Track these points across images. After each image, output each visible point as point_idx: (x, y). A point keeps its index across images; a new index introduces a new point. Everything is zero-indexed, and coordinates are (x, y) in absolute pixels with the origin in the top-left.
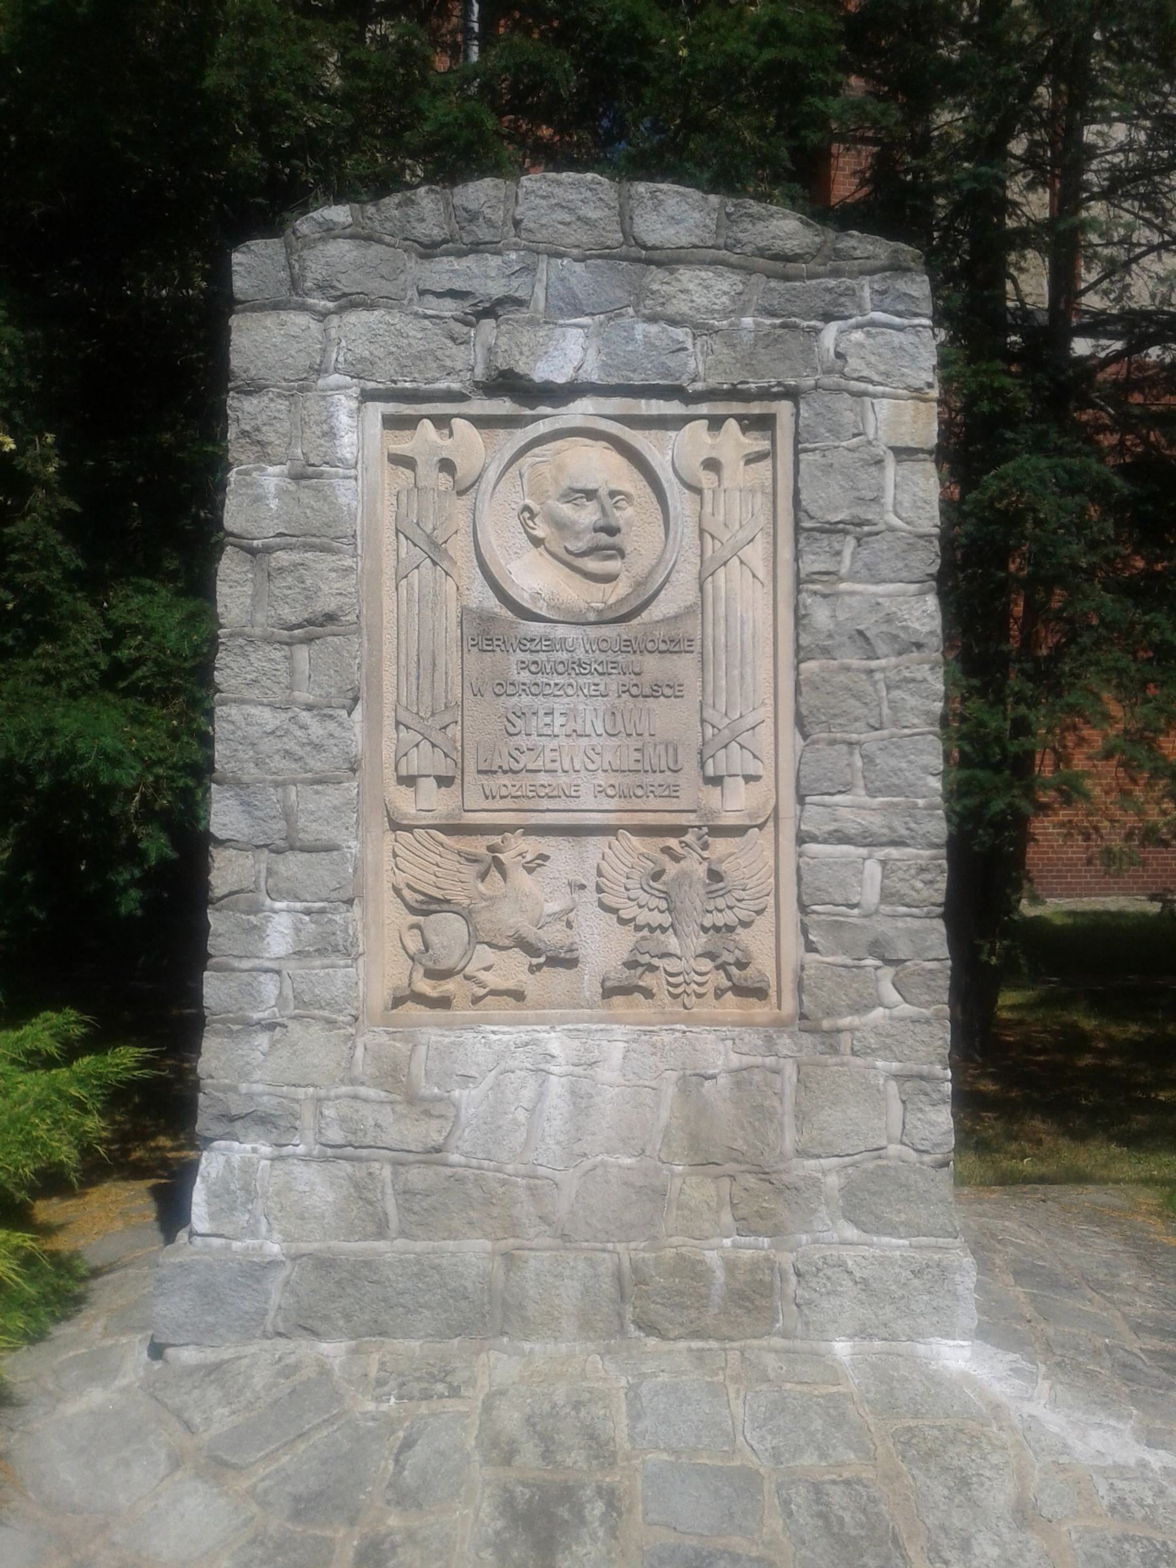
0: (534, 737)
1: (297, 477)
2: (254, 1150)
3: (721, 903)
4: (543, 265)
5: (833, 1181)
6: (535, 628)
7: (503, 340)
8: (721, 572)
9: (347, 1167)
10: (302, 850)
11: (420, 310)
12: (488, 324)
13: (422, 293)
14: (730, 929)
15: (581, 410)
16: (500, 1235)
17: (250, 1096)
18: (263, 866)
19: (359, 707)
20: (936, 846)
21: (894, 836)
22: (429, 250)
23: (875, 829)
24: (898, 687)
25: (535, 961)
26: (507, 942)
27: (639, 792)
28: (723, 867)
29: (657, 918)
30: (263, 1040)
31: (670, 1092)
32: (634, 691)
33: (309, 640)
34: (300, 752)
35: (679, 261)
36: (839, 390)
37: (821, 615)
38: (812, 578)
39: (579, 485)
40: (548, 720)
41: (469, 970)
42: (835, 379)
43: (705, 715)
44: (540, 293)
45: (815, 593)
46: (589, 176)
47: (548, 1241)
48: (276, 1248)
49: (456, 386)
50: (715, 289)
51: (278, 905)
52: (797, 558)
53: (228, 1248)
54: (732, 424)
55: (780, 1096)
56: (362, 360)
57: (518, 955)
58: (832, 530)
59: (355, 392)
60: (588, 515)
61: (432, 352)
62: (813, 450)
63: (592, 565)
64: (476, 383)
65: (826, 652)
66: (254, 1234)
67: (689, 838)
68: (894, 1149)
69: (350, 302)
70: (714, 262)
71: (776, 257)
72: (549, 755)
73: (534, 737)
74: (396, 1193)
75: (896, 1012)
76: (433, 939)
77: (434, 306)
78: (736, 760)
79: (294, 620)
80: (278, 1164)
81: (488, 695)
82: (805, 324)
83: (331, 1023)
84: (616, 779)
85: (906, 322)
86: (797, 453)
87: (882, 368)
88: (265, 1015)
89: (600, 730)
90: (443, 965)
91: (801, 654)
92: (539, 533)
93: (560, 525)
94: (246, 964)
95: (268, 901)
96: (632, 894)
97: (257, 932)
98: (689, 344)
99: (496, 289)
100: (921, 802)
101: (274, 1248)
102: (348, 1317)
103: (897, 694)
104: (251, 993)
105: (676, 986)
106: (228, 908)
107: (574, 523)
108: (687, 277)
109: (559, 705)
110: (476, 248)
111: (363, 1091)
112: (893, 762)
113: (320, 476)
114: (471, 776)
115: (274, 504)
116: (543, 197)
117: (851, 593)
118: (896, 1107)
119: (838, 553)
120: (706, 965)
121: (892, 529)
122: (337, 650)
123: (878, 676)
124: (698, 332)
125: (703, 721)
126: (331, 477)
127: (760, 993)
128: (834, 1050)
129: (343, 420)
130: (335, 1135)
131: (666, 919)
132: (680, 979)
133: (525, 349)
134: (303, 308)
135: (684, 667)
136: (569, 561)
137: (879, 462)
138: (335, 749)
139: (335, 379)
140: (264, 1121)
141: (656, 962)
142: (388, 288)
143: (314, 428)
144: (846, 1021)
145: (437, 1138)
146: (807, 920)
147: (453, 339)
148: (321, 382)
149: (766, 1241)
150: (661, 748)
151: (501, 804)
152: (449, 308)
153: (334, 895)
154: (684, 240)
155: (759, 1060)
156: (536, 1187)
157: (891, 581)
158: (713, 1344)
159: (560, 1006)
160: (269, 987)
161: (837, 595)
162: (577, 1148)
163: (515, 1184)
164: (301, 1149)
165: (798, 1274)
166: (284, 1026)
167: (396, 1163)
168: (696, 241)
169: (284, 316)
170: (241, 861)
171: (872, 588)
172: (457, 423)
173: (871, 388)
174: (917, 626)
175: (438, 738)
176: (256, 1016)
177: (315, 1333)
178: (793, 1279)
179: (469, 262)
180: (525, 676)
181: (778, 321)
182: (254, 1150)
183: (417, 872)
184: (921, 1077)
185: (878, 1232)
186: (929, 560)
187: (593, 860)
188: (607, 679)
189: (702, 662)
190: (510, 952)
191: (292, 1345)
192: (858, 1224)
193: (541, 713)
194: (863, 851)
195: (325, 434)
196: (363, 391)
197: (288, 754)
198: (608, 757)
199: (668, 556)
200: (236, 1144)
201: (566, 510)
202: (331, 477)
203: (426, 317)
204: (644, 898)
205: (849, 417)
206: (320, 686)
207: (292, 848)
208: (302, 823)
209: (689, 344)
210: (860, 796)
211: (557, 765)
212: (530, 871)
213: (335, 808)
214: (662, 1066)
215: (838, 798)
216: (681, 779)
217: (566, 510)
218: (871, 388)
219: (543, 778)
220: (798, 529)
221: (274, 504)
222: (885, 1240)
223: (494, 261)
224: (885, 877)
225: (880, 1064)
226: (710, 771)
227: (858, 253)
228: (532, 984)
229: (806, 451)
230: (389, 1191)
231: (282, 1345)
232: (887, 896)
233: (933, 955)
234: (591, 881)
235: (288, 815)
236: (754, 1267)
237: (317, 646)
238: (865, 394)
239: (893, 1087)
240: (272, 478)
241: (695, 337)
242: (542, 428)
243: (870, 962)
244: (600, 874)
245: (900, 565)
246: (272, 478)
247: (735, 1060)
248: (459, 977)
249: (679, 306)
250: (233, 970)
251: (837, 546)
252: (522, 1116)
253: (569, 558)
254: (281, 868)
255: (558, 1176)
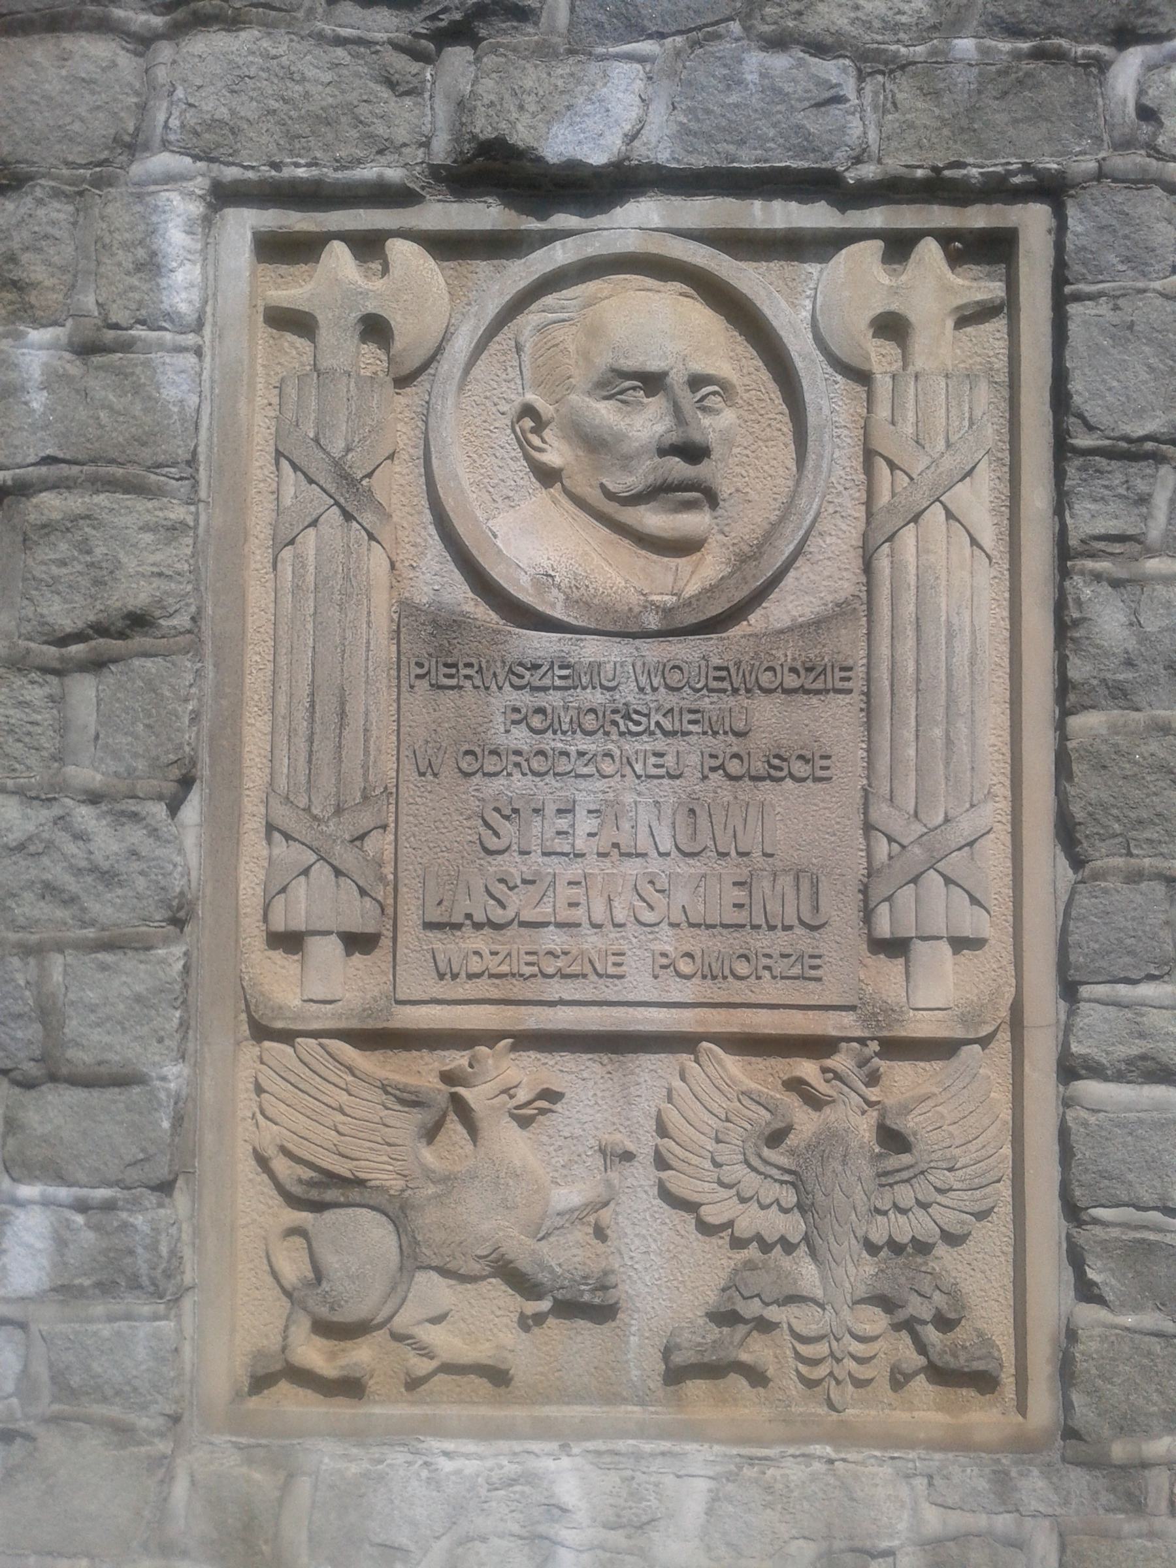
0: (536, 858)
1: (86, 349)
3: (905, 1195)
6: (541, 644)
8: (908, 535)
11: (328, 29)
12: (458, 56)
14: (922, 1248)
25: (532, 1307)
26: (476, 1268)
27: (742, 968)
28: (909, 1124)
32: (734, 767)
33: (97, 665)
34: (71, 884)
36: (1141, 182)
38: (1092, 547)
39: (630, 364)
40: (563, 823)
41: (401, 1322)
42: (1137, 160)
45: (1098, 577)
49: (394, 174)
51: (27, 1191)
52: (1061, 503)
54: (930, 250)
56: (214, 124)
57: (498, 1292)
59: (200, 185)
61: (350, 108)
65: (1120, 694)
67: (841, 1061)
72: (565, 893)
73: (536, 858)
76: (331, 1260)
79: (68, 625)
81: (448, 773)
82: (1080, 49)
83: (123, 1432)
84: (699, 942)
89: (666, 845)
90: (351, 1313)
98: (849, 88)
105: (814, 1362)
107: (620, 437)
109: (587, 794)
113: (127, 346)
115: (38, 401)
119: (1144, 500)
120: (874, 1321)
124: (867, 67)
125: (868, 827)
126: (148, 348)
127: (984, 1382)
128: (1135, 1504)
131: (793, 1226)
132: (821, 1349)
134: (103, 26)
138: (141, 883)
141: (773, 1313)
146: (1083, 1237)
147: (391, 84)
148: (137, 170)
150: (786, 881)
153: (133, 1174)
155: (981, 1521)
161: (1141, 581)
166: (28, 1437)
169: (69, 42)
172: (401, 251)
175: (347, 857)
180: (520, 737)
181: (1025, 46)
183: (302, 1123)
188: (680, 744)
189: (869, 711)
190: (483, 1286)
193: (551, 809)
195: (139, 267)
197: (49, 890)
198: (681, 897)
199: (803, 502)
202: (148, 348)
204: (750, 1182)
206: (116, 755)
207: (53, 1078)
208: (73, 1026)
209: (849, 88)
211: (579, 914)
212: (524, 1122)
213: (138, 999)
215: (1147, 990)
216: (826, 943)
219: (553, 939)
220: (1062, 449)
221: (38, 401)
226: (884, 928)
229: (1078, 298)
234: (644, 1143)
237: (113, 675)
241: (861, 77)
242: (560, 255)
244: (662, 1130)
247: (933, 1520)
248: (381, 1335)
251: (1141, 486)
253: (610, 508)
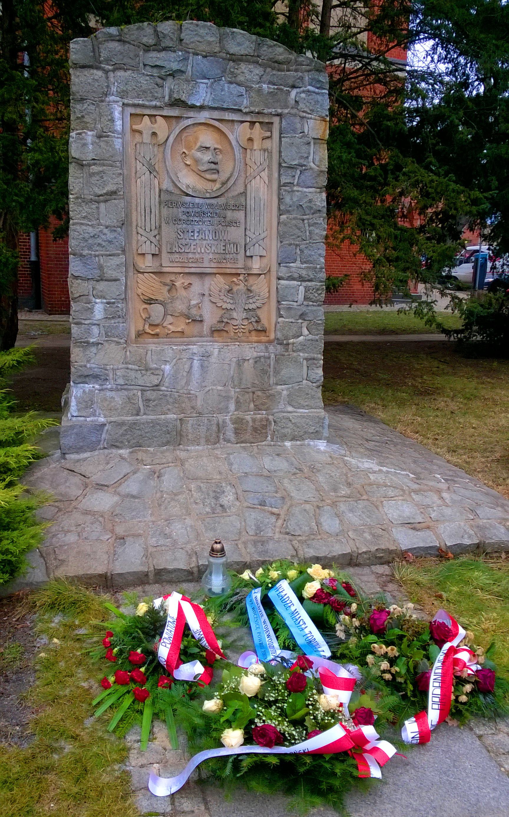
0: (188, 240)
1: (99, 137)
2: (93, 387)
3: (251, 301)
4: (191, 58)
5: (285, 393)
6: (188, 199)
7: (176, 87)
8: (253, 181)
9: (126, 393)
10: (106, 280)
11: (145, 73)
12: (170, 79)
13: (145, 65)
14: (254, 310)
15: (204, 116)
16: (179, 413)
17: (91, 368)
18: (90, 286)
19: (124, 227)
20: (321, 282)
21: (309, 278)
22: (147, 48)
23: (303, 275)
24: (312, 226)
25: (187, 321)
26: (178, 315)
27: (225, 261)
28: (252, 288)
29: (229, 306)
30: (94, 349)
31: (233, 365)
32: (223, 224)
33: (106, 201)
34: (104, 244)
35: (241, 60)
36: (295, 115)
37: (287, 199)
38: (285, 185)
39: (204, 145)
40: (192, 234)
41: (164, 325)
42: (294, 111)
43: (247, 233)
44: (189, 68)
45: (285, 191)
46: (209, 24)
47: (195, 415)
48: (103, 419)
49: (158, 104)
50: (254, 73)
51: (98, 301)
52: (280, 175)
53: (86, 420)
54: (257, 124)
55: (269, 365)
56: (123, 91)
57: (182, 319)
58: (291, 167)
59: (121, 104)
60: (207, 157)
61: (149, 89)
62: (287, 137)
63: (208, 176)
64: (165, 103)
65: (288, 212)
66: (94, 415)
67: (241, 277)
68: (305, 382)
69: (117, 68)
70: (254, 62)
71: (276, 62)
72: (192, 247)
73: (188, 240)
74: (143, 401)
75: (307, 338)
76: (152, 314)
77: (148, 71)
78: (257, 250)
79: (100, 193)
80: (101, 392)
81: (171, 224)
82: (285, 89)
83: (118, 343)
84: (217, 256)
85: (320, 91)
86: (280, 138)
87: (311, 108)
88: (94, 340)
89: (211, 238)
90: (156, 322)
91: (281, 213)
92: (188, 163)
93: (197, 161)
94: (87, 322)
95: (94, 299)
96: (221, 298)
97: (91, 310)
98: (244, 93)
99: (175, 66)
100: (318, 266)
101: (102, 419)
102: (129, 442)
103: (311, 228)
104: (88, 332)
105: (236, 329)
106: (78, 301)
107: (202, 159)
108: (243, 66)
109: (197, 228)
110: (165, 49)
111: (130, 366)
112: (309, 252)
113: (108, 136)
114: (164, 255)
115: (91, 147)
116: (192, 31)
117: (298, 191)
118: (305, 368)
119: (294, 176)
120: (246, 322)
121: (311, 169)
122: (116, 206)
123: (306, 221)
124: (248, 89)
125: (246, 235)
126: (112, 137)
127: (264, 331)
128: (287, 350)
129: (117, 114)
130: (121, 381)
131: (232, 307)
132: (237, 327)
133: (185, 91)
134: (98, 68)
135: (240, 215)
136: (200, 174)
137: (309, 143)
138: (117, 243)
139: (112, 98)
140: (96, 377)
141: (229, 321)
142: (133, 63)
143: (105, 117)
144: (291, 341)
145: (156, 382)
146: (280, 307)
147: (157, 84)
148: (107, 99)
149: (264, 412)
150: (232, 245)
151: (175, 265)
152: (155, 72)
153: (118, 297)
154: (242, 52)
155: (262, 354)
156: (190, 397)
157: (311, 187)
158: (249, 445)
159: (195, 337)
160: (95, 330)
161: (293, 191)
162: (203, 384)
163: (183, 396)
164: (109, 386)
165: (275, 422)
166: (102, 344)
167: (142, 390)
168: (247, 53)
169: (92, 71)
170: (83, 284)
171: (305, 190)
172: (159, 119)
173: (307, 115)
174: (319, 204)
175: (153, 240)
176: (92, 340)
177: (117, 447)
178: (273, 423)
179: (163, 54)
180: (184, 217)
181: (276, 87)
182: (93, 387)
183: (145, 289)
184: (314, 359)
185: (299, 408)
186: (323, 181)
187: (207, 286)
188: (213, 219)
189: (246, 214)
190: (179, 318)
191: (110, 451)
192: (293, 406)
193: (190, 231)
194: (299, 283)
195: (109, 120)
196: (123, 104)
197: (99, 244)
198: (213, 248)
199: (235, 174)
200: (87, 385)
201: (199, 155)
202: (112, 137)
203: (148, 75)
204: (225, 299)
205: (298, 126)
206: (110, 219)
207: (102, 280)
208: (105, 270)
209: (244, 93)
210: (298, 264)
211: (195, 251)
212: (185, 288)
213: (118, 265)
214: (231, 357)
215: (292, 265)
216: (239, 257)
217: (199, 155)
218: (307, 115)
219: (190, 256)
220: (280, 165)
221: (91, 147)
222: (301, 410)
223: (173, 55)
224: (306, 292)
225: (301, 354)
226: (248, 254)
227: (304, 63)
228: (188, 330)
229: (284, 137)
230: (140, 399)
231: (106, 451)
232: (306, 298)
233: (320, 318)
234: (207, 293)
235: (101, 267)
236: (261, 420)
237: (108, 203)
238: (305, 117)
239: (305, 361)
240: (90, 136)
241: (246, 91)
242: (189, 122)
243: (300, 321)
244: (210, 290)
245: (314, 181)
246: (90, 136)
247: (255, 354)
248: (160, 327)
249: (241, 78)
250: (82, 324)
251: (294, 174)
252: (185, 374)
253: (199, 173)
254: (97, 287)
255: (197, 394)
